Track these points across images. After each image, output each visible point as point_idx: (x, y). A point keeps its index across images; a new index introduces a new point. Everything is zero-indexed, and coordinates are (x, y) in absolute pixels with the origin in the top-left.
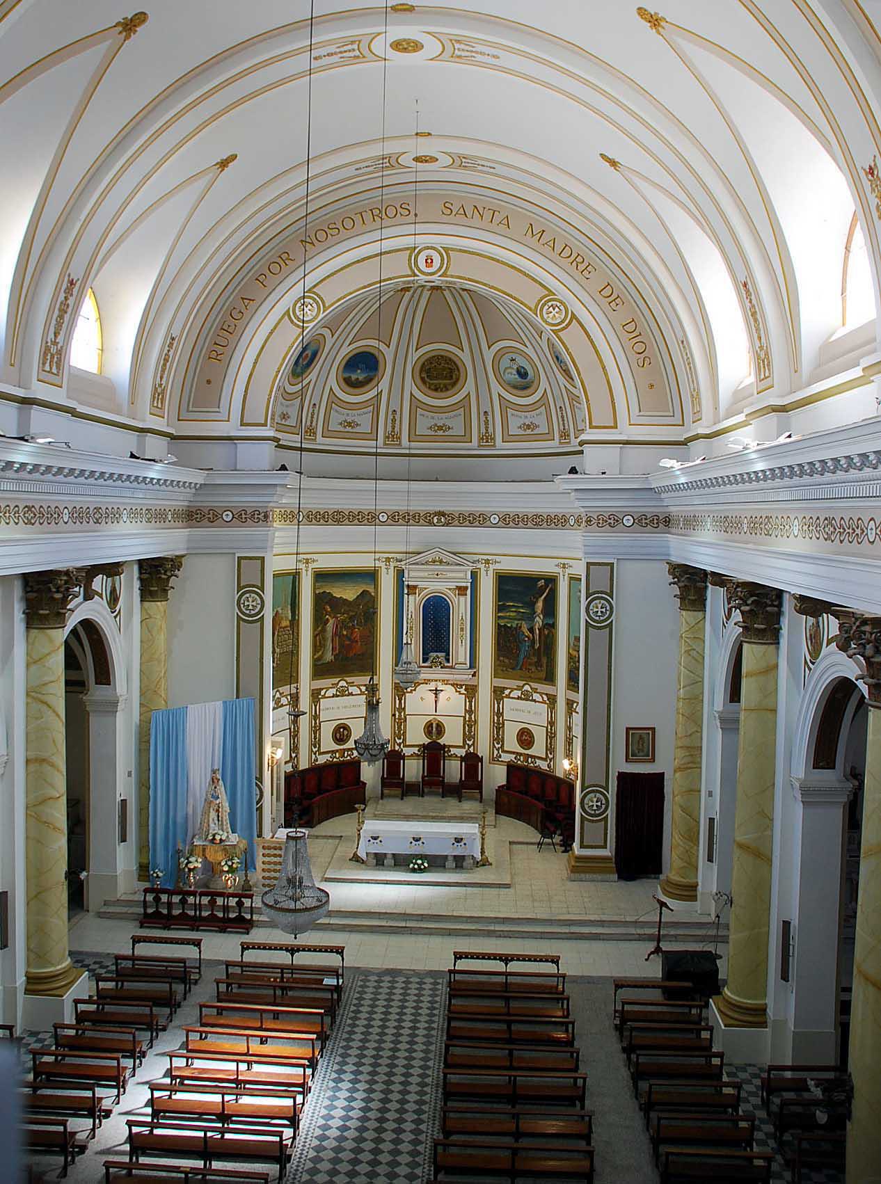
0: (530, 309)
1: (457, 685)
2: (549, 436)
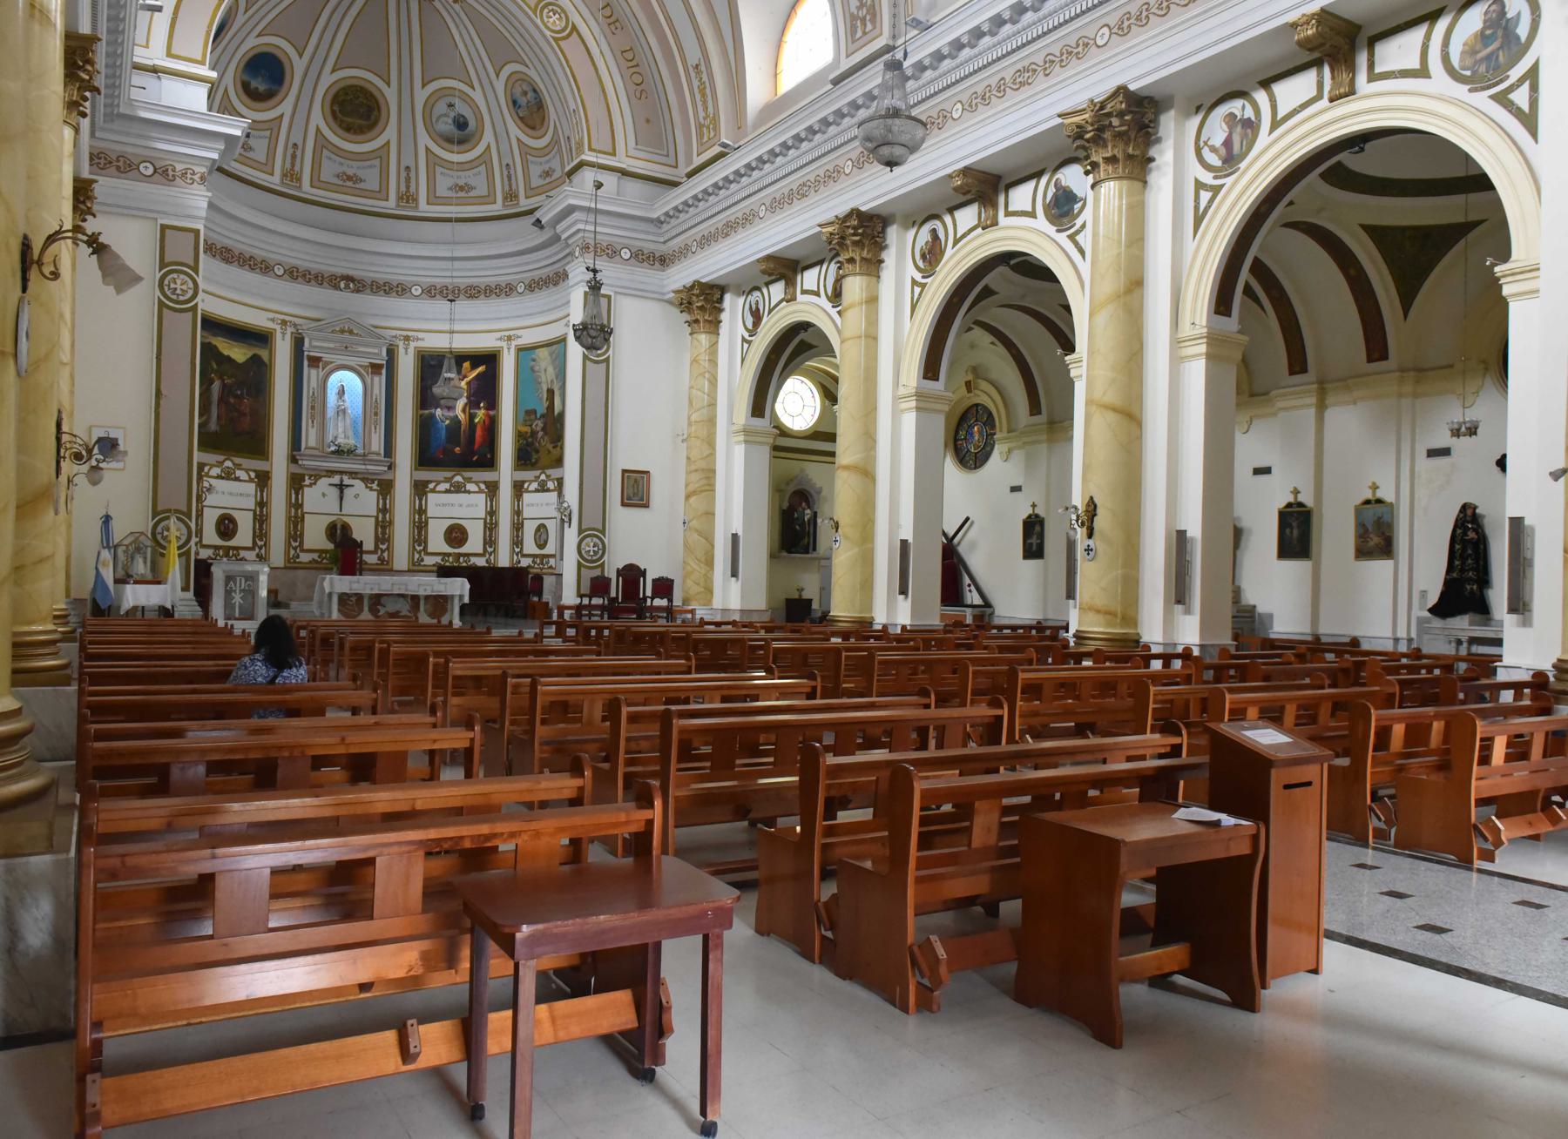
0: (530, 8)
1: (367, 479)
2: (489, 198)
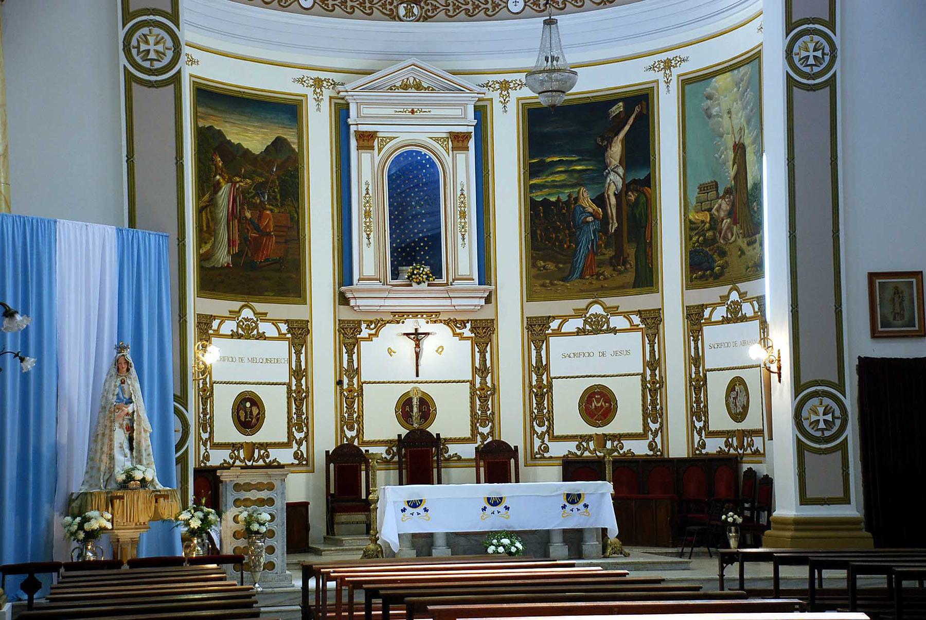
1: (455, 321)
